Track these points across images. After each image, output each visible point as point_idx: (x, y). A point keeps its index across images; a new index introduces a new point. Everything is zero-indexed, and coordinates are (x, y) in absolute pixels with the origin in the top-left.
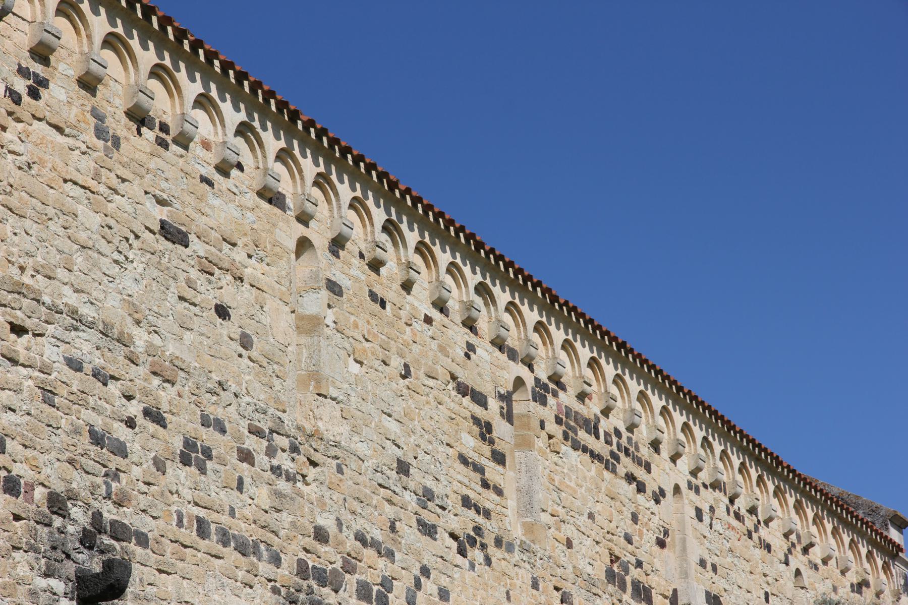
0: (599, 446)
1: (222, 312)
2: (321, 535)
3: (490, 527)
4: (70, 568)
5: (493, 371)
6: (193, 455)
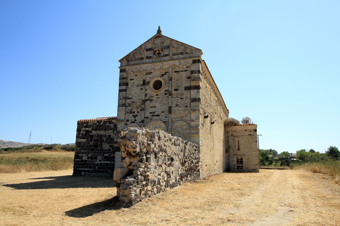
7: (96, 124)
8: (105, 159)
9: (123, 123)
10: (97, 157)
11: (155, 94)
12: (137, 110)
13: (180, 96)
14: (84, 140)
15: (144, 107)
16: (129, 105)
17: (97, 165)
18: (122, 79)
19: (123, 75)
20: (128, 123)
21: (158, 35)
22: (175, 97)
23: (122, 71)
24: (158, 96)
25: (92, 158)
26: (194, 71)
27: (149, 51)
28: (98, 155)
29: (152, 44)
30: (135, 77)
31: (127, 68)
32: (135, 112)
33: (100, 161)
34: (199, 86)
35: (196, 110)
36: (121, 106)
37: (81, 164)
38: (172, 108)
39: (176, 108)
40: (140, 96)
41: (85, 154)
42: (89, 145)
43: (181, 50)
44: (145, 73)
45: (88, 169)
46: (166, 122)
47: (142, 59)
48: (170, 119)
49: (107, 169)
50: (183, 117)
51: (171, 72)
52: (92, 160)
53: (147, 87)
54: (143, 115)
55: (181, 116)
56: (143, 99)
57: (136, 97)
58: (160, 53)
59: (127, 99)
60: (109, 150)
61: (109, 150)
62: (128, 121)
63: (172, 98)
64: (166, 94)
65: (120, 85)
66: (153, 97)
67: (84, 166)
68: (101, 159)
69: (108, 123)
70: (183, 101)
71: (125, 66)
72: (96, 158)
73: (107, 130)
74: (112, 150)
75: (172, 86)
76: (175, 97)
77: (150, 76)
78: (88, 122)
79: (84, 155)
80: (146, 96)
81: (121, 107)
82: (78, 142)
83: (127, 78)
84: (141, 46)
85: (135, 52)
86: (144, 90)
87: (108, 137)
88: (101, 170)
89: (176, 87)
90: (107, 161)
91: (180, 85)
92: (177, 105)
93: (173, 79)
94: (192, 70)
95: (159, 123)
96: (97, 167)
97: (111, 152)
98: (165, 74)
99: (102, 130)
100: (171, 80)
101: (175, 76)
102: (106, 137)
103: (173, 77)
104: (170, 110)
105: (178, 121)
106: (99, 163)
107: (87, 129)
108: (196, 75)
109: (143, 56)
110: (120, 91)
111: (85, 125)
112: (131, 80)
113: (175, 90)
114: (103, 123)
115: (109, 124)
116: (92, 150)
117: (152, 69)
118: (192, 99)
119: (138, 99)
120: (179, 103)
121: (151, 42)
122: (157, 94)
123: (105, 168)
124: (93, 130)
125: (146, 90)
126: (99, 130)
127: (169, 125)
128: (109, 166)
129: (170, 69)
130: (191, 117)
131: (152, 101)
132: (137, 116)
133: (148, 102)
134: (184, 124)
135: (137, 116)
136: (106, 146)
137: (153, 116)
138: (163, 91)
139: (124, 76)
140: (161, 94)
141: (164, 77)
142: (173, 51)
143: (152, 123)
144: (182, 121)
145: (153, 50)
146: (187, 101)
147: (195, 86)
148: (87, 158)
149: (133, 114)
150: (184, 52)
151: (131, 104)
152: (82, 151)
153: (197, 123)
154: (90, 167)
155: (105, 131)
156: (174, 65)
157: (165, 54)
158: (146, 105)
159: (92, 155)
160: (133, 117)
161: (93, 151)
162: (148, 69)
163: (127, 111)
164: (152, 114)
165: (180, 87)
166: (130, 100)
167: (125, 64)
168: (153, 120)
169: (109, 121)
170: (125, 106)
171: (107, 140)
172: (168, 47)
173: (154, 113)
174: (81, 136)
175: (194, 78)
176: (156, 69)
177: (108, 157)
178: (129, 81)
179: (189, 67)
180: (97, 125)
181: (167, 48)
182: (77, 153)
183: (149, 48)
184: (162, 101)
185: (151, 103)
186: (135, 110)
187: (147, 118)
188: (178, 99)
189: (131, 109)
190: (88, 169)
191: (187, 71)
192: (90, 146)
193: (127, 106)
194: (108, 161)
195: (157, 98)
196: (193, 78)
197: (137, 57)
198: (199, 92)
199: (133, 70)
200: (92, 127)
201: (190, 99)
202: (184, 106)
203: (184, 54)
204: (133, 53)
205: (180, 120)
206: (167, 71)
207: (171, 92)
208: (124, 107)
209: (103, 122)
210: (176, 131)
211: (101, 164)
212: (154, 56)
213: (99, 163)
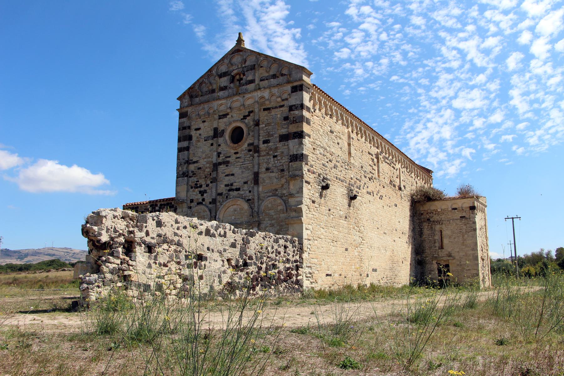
0: (388, 162)
1: (338, 144)
2: (352, 179)
3: (374, 176)
4: (321, 185)
5: (374, 150)
6: (335, 167)
11: (233, 151)
16: (193, 174)
22: (264, 156)
23: (182, 115)
24: (238, 155)
26: (295, 105)
30: (201, 125)
31: (189, 110)
34: (302, 132)
38: (260, 175)
39: (265, 175)
40: (209, 157)
44: (216, 117)
46: (249, 200)
47: (213, 91)
48: (256, 194)
50: (276, 190)
51: (256, 110)
53: (221, 140)
54: (214, 190)
55: (273, 188)
56: (215, 162)
57: (204, 159)
58: (242, 79)
59: (190, 163)
62: (192, 201)
64: (250, 151)
65: (179, 140)
66: (229, 157)
75: (259, 136)
76: (264, 156)
77: (225, 120)
80: (219, 156)
83: (189, 127)
84: (210, 70)
85: (201, 81)
86: (215, 145)
93: (261, 123)
94: (290, 104)
95: (239, 203)
98: (249, 115)
101: (264, 116)
103: (261, 119)
105: (269, 196)
108: (296, 112)
109: (215, 87)
110: (180, 150)
112: (197, 130)
113: (265, 142)
118: (290, 156)
119: (207, 163)
120: (270, 166)
122: (236, 151)
129: (256, 106)
131: (229, 165)
132: (205, 191)
133: (222, 168)
135: (205, 191)
137: (230, 190)
138: (246, 145)
139: (185, 125)
140: (242, 150)
141: (246, 121)
142: (261, 73)
145: (229, 75)
146: (284, 161)
147: (295, 133)
149: (199, 189)
150: (278, 74)
153: (298, 199)
156: (262, 97)
162: (222, 108)
164: (228, 188)
165: (272, 135)
166: (196, 165)
167: (186, 104)
170: (187, 176)
172: (253, 68)
173: (232, 185)
175: (295, 119)
178: (193, 133)
179: (287, 99)
181: (251, 70)
186: (202, 182)
187: (221, 194)
188: (268, 157)
189: (196, 180)
196: (292, 119)
197: (205, 89)
198: (301, 143)
202: (278, 169)
203: (278, 77)
204: (198, 84)
205: (272, 196)
206: (251, 110)
207: (258, 146)
208: (186, 178)
209: (159, 206)
212: (232, 85)
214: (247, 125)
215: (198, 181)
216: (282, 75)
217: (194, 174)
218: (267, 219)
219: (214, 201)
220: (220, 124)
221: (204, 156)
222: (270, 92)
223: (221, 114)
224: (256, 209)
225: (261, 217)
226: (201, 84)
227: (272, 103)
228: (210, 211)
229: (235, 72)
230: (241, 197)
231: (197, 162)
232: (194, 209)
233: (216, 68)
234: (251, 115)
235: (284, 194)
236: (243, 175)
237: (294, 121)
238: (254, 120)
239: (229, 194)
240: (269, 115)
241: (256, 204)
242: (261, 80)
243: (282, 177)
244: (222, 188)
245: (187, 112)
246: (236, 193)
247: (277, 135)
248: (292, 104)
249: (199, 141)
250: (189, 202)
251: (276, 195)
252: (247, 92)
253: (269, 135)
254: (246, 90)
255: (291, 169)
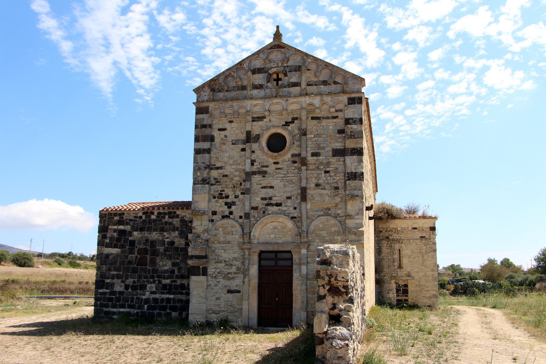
7: (141, 217)
8: (162, 289)
9: (205, 218)
10: (146, 286)
11: (272, 161)
12: (234, 191)
13: (322, 167)
14: (115, 251)
15: (249, 187)
16: (216, 182)
17: (147, 301)
18: (201, 128)
19: (204, 119)
20: (214, 217)
21: (276, 43)
23: (200, 110)
24: (279, 166)
25: (134, 288)
26: (352, 119)
27: (258, 73)
28: (147, 281)
29: (264, 60)
30: (228, 126)
31: (211, 105)
32: (230, 197)
33: (152, 293)
35: (357, 196)
36: (200, 182)
37: (110, 300)
38: (308, 191)
39: (315, 192)
40: (239, 164)
41: (118, 278)
42: (127, 260)
43: (324, 75)
44: (249, 118)
45: (127, 310)
47: (244, 88)
49: (168, 311)
50: (329, 209)
51: (304, 118)
52: (134, 292)
53: (255, 146)
55: (325, 207)
57: (231, 165)
58: (281, 80)
59: (212, 169)
60: (173, 272)
61: (173, 272)
62: (214, 213)
63: (307, 170)
64: (295, 162)
65: (197, 139)
66: (267, 166)
67: (118, 303)
68: (154, 289)
69: (167, 217)
70: (329, 178)
71: (207, 101)
72: (143, 287)
73: (166, 232)
74: (178, 272)
75: (307, 147)
77: (260, 123)
78: (123, 214)
79: (115, 280)
81: (200, 186)
82: (103, 253)
83: (210, 126)
84: (240, 63)
85: (227, 73)
86: (248, 151)
87: (168, 244)
88: (155, 312)
89: (316, 148)
90: (167, 293)
91: (322, 145)
92: (317, 185)
93: (308, 133)
94: (347, 116)
95: (280, 220)
96: (146, 306)
97: (177, 275)
98: (292, 122)
99: (155, 230)
100: (305, 134)
101: (312, 125)
102: (164, 244)
103: (308, 128)
104: (304, 195)
105: (320, 216)
106: (151, 297)
107: (121, 227)
108: (354, 127)
109: (245, 83)
110: (197, 152)
111: (116, 218)
112: (220, 130)
113: (313, 155)
114: (157, 217)
115: (169, 217)
116: (134, 271)
117: (265, 110)
118: (348, 173)
119: (237, 170)
120: (321, 181)
121: (261, 55)
123: (164, 308)
124: (134, 229)
125: (253, 152)
126: (147, 231)
127: (302, 223)
128: (173, 303)
130: (346, 208)
131: (266, 175)
132: (234, 203)
133: (256, 178)
134: (334, 222)
135: (234, 203)
136: (165, 265)
137: (268, 205)
138: (289, 156)
139: (205, 123)
140: (284, 161)
141: (289, 128)
142: (306, 77)
143: (265, 220)
144: (328, 217)
145: (265, 72)
146: (338, 178)
147: (354, 149)
148: (123, 287)
149: (225, 200)
150: (331, 81)
151: (220, 179)
152: (112, 273)
153: (358, 221)
154: (130, 307)
155: (161, 234)
156: (311, 104)
157: (291, 81)
158: (252, 181)
159: (134, 282)
160: (226, 207)
161: (136, 272)
162: (256, 109)
163: (211, 194)
164: (266, 202)
165: (323, 148)
166: (220, 171)
167: (206, 98)
168: (269, 212)
169: (169, 213)
170: (208, 183)
171: (166, 250)
172: (298, 69)
173: (270, 198)
174: (108, 241)
176: (274, 112)
177: (170, 285)
178: (216, 133)
180: (144, 221)
181: (296, 71)
182: (101, 277)
183: (257, 67)
184: (286, 176)
185: (263, 178)
186: (228, 191)
187: (256, 208)
188: (319, 172)
189: (220, 189)
190: (127, 310)
191: (336, 117)
192: (130, 262)
193: (212, 183)
194: (169, 293)
195: (276, 169)
196: (349, 133)
197: (232, 84)
199: (224, 109)
200: (131, 223)
201: (343, 174)
202: (331, 187)
203: (329, 84)
204: (223, 77)
205: (323, 215)
206: (295, 116)
207: (305, 158)
208: (207, 186)
210: (317, 235)
211: (155, 300)
212: (269, 85)
213: (151, 297)
214: (290, 133)
215: (224, 191)
216: (335, 83)
217: (217, 181)
218: (317, 240)
219: (247, 216)
220: (254, 127)
221: (231, 162)
222: (322, 100)
223: (255, 116)
224: (304, 228)
225: (310, 238)
226: (227, 77)
227: (323, 113)
228: (241, 226)
229: (274, 70)
230: (284, 213)
231: (221, 168)
232: (219, 223)
233: (248, 62)
234: (296, 122)
235: (338, 214)
236: (286, 189)
237: (351, 135)
238: (300, 129)
239: (266, 210)
240: (319, 125)
241: (305, 224)
242: (308, 85)
243: (336, 195)
244: (257, 201)
245: (207, 108)
246: (276, 208)
247: (329, 149)
248: (348, 117)
249: (224, 144)
250: (211, 214)
251: (330, 215)
252: (289, 96)
253: (319, 147)
254: (289, 93)
255: (348, 188)
